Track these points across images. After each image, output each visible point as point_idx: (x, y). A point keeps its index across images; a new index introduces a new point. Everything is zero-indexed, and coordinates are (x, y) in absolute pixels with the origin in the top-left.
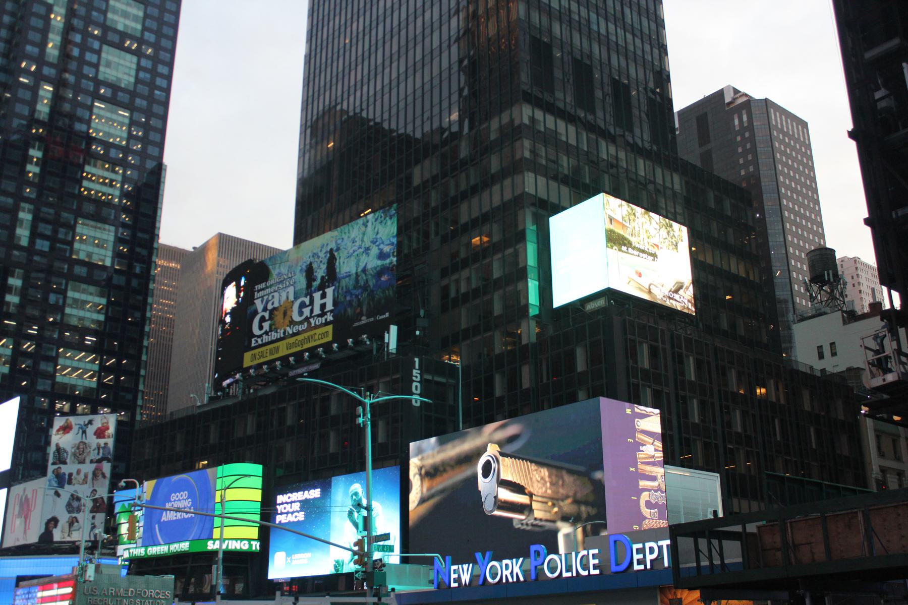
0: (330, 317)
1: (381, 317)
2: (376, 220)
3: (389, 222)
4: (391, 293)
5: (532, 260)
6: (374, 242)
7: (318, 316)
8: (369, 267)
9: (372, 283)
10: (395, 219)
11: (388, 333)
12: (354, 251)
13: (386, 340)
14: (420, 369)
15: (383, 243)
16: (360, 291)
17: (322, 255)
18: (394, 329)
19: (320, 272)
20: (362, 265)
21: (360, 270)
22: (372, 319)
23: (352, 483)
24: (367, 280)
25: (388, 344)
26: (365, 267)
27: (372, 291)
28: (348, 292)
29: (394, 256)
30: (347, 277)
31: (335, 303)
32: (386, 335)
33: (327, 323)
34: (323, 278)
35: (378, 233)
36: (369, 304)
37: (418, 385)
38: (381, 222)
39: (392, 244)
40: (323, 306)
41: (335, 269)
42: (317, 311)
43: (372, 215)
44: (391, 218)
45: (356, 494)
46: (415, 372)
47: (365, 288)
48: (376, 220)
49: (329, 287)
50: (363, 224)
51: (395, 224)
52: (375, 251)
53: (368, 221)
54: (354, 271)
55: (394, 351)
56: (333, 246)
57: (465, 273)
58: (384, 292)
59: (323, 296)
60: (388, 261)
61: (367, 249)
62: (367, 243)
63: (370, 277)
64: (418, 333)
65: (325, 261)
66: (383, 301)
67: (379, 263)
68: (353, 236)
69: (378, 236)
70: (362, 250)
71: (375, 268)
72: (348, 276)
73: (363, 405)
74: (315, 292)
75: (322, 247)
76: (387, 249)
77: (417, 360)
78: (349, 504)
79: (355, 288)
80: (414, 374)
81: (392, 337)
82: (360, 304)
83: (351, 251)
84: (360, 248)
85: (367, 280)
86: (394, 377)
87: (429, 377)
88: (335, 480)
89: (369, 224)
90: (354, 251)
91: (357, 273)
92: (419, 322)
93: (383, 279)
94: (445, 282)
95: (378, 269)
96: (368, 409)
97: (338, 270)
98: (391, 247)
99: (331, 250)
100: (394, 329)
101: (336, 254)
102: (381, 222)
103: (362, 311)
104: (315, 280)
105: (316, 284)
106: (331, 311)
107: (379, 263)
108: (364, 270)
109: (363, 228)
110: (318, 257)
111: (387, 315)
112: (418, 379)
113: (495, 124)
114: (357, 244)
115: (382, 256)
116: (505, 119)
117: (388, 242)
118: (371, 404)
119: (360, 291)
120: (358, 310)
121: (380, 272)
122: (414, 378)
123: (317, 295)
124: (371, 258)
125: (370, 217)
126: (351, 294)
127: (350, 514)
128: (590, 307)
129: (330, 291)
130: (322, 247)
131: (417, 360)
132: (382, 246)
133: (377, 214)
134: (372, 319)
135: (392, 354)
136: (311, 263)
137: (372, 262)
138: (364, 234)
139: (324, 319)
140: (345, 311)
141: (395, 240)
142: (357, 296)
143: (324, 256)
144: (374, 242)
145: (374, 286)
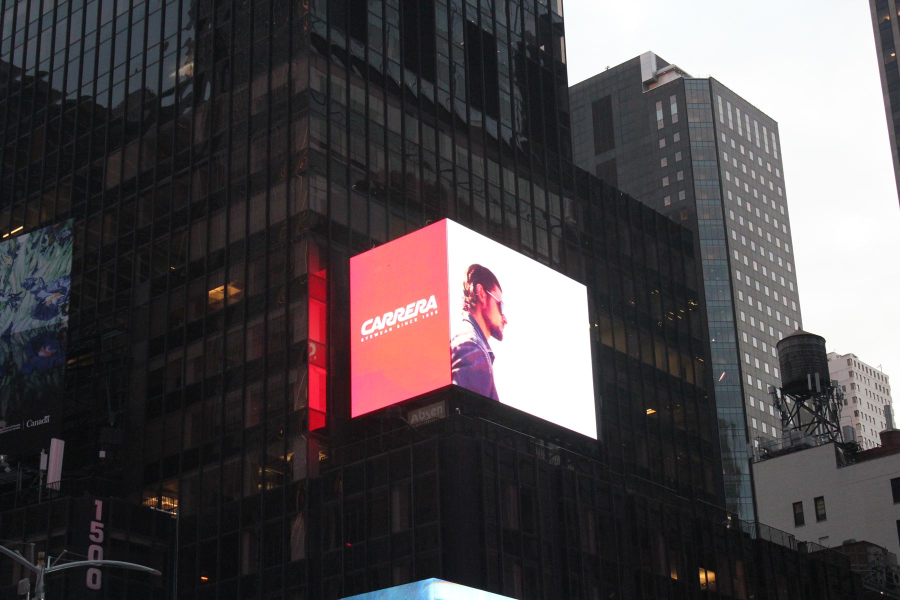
1: (34, 424)
2: (34, 246)
3: (58, 252)
6: (27, 286)
8: (16, 330)
9: (18, 361)
10: (69, 246)
11: (48, 452)
13: (43, 466)
18: (57, 446)
22: (17, 427)
25: (46, 472)
26: (9, 329)
29: (64, 313)
32: (44, 457)
35: (36, 270)
37: (100, 549)
38: (43, 250)
39: (64, 289)
43: (27, 236)
44: (62, 245)
46: (94, 524)
48: (34, 246)
50: (9, 252)
51: (70, 255)
52: (28, 301)
53: (18, 248)
55: (57, 487)
57: (196, 350)
60: (53, 321)
61: (15, 299)
63: (17, 348)
64: (102, 454)
67: (36, 323)
69: (37, 276)
70: (5, 299)
71: (28, 333)
73: (33, 576)
76: (52, 299)
77: (99, 503)
80: (93, 529)
81: (54, 460)
86: (55, 534)
87: (119, 536)
89: (21, 253)
93: (41, 354)
95: (33, 335)
96: (42, 584)
98: (59, 296)
100: (57, 446)
102: (43, 250)
107: (36, 323)
109: (9, 260)
111: (47, 419)
112: (100, 539)
113: (260, 88)
115: (41, 311)
116: (280, 79)
117: (56, 287)
118: (48, 576)
121: (37, 340)
122: (92, 537)
124: (21, 313)
125: (23, 239)
128: (417, 417)
131: (99, 503)
132: (42, 294)
133: (37, 234)
134: (17, 427)
135: (53, 491)
137: (23, 322)
138: (10, 270)
141: (67, 284)
144: (27, 286)
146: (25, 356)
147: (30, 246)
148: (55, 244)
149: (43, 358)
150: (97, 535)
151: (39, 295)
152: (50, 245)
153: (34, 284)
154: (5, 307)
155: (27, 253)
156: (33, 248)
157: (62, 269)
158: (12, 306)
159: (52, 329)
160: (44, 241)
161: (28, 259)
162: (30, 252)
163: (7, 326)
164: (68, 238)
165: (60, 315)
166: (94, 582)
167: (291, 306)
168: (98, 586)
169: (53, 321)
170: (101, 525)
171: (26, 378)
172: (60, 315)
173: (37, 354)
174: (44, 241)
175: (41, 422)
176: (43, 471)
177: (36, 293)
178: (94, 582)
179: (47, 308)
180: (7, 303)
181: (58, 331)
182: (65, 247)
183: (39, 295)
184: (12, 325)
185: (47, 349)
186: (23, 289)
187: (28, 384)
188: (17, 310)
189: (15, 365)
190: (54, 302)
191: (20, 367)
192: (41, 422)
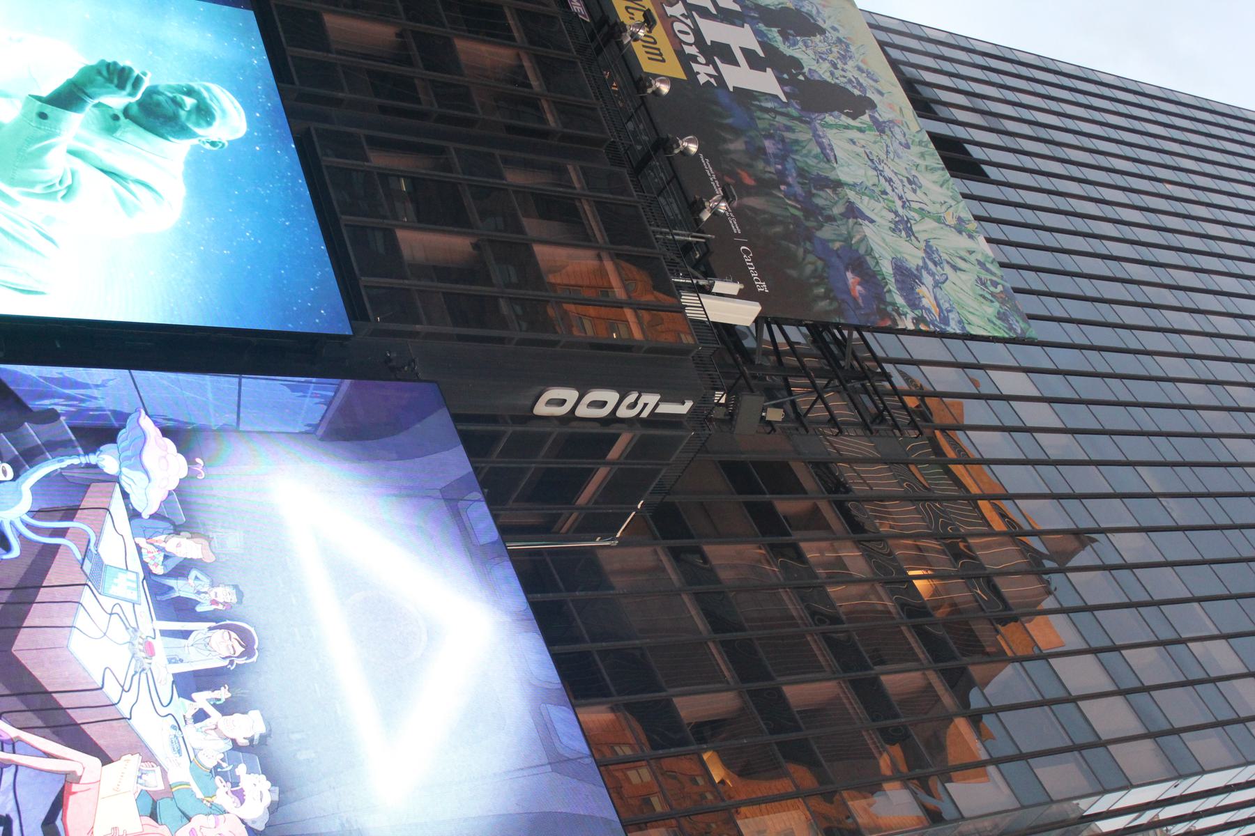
0: (703, 72)
1: (748, 260)
3: (991, 310)
4: (823, 304)
5: (711, 686)
6: (929, 250)
7: (697, 32)
8: (868, 229)
9: (826, 233)
11: (742, 295)
12: (889, 181)
13: (719, 286)
14: (657, 420)
15: (937, 284)
16: (799, 190)
17: (852, 73)
19: (809, 57)
20: (865, 204)
21: (852, 195)
22: (736, 229)
23: (240, 93)
24: (831, 219)
25: (707, 290)
27: (810, 237)
28: (788, 149)
30: (821, 145)
31: (744, 96)
33: (686, 61)
34: (797, 64)
35: (955, 268)
36: (773, 221)
40: (721, 52)
41: (829, 109)
42: (714, 31)
45: (204, 112)
46: (651, 399)
47: (812, 211)
49: (781, 82)
50: (960, 219)
53: (970, 236)
54: (843, 174)
56: (884, 114)
58: (820, 278)
59: (754, 62)
60: (900, 300)
61: (903, 226)
62: (924, 228)
65: (841, 81)
66: (793, 273)
68: (926, 180)
69: (948, 270)
70: (900, 211)
71: (870, 252)
72: (827, 155)
74: (757, 33)
75: (869, 75)
77: (684, 408)
78: (159, 74)
79: (802, 173)
81: (728, 306)
82: (765, 186)
83: (888, 173)
84: (905, 204)
85: (831, 219)
87: (614, 453)
88: (251, 14)
90: (889, 181)
91: (838, 184)
92: (751, 402)
93: (849, 275)
94: (807, 479)
95: (871, 263)
97: (829, 119)
99: (873, 106)
101: (866, 118)
103: (746, 191)
104: (785, 37)
105: (774, 34)
106: (720, 78)
107: (887, 268)
108: (852, 212)
110: (844, 58)
114: (910, 195)
115: (907, 278)
117: (946, 306)
119: (799, 190)
120: (749, 181)
122: (632, 397)
123: (741, 38)
124: (890, 238)
126: (783, 157)
127: (118, 76)
129: (766, 82)
130: (869, 75)
131: (684, 408)
132: (928, 279)
134: (736, 229)
136: (822, 31)
138: (939, 220)
139: (692, 50)
140: (737, 132)
142: (782, 177)
143: (847, 75)
144: (929, 250)
145: (824, 242)
146: (837, 245)
147: (980, 257)
148: (997, 304)
149: (845, 280)
150: (633, 406)
151: (924, 273)
152: (992, 294)
153: (935, 264)
154: (891, 211)
155: (971, 252)
156: (979, 263)
157: (970, 317)
158: (896, 222)
159: (888, 299)
160: (995, 284)
161: (964, 254)
162: (972, 258)
163: (868, 213)
164: (1011, 328)
165: (911, 315)
166: (550, 402)
167: (991, 769)
168: (541, 409)
169: (900, 300)
170: (645, 414)
171: (808, 245)
172: (911, 315)
173: (847, 269)
174: (995, 284)
175: (755, 275)
176: (712, 286)
177: (926, 267)
178: (550, 402)
179: (913, 289)
180: (896, 213)
181: (889, 309)
182: (998, 322)
183: (924, 273)
184: (872, 221)
185: (859, 288)
186: (923, 245)
187: (801, 251)
188: (893, 230)
189: (821, 227)
190: (925, 302)
191: (819, 234)
192: (755, 275)
